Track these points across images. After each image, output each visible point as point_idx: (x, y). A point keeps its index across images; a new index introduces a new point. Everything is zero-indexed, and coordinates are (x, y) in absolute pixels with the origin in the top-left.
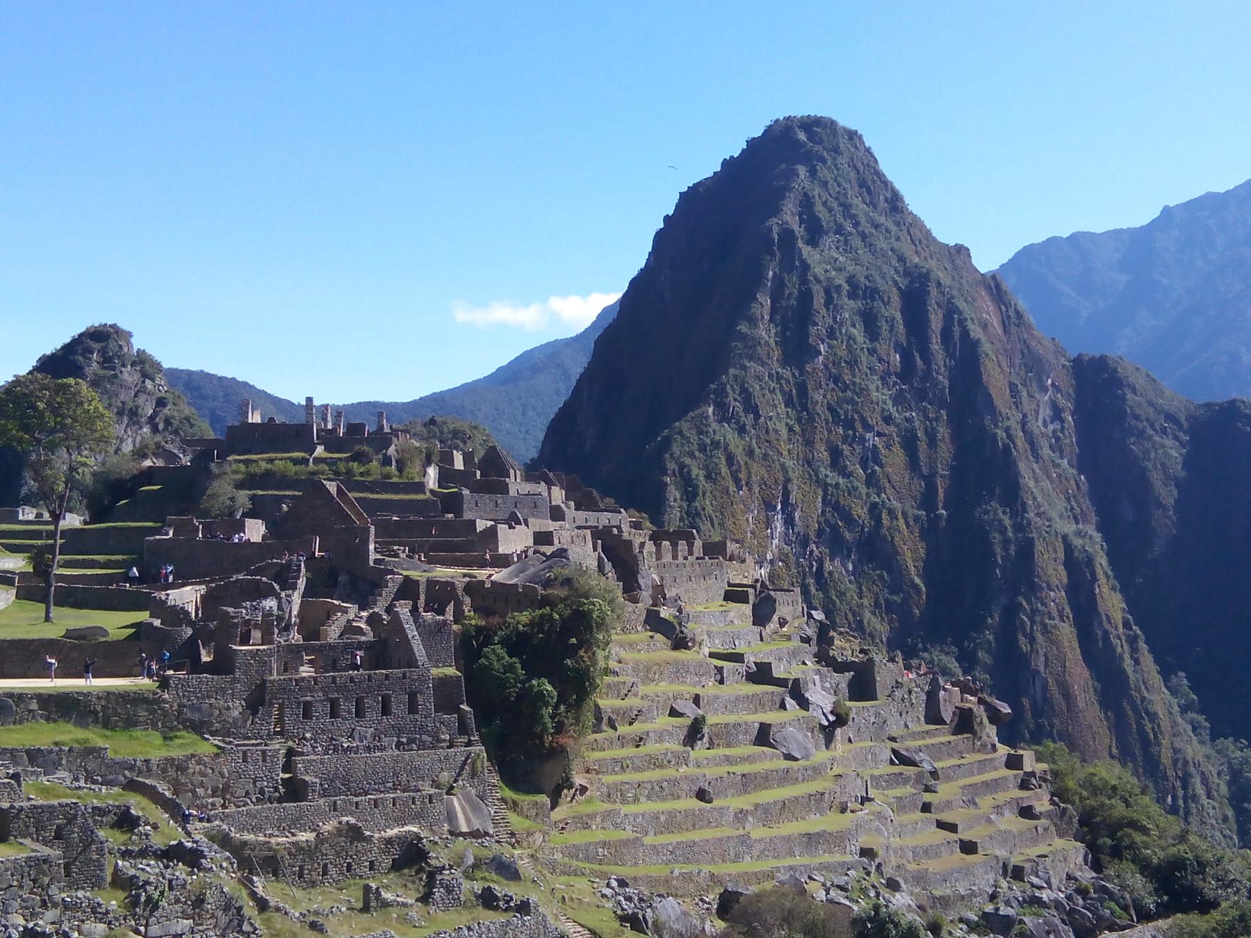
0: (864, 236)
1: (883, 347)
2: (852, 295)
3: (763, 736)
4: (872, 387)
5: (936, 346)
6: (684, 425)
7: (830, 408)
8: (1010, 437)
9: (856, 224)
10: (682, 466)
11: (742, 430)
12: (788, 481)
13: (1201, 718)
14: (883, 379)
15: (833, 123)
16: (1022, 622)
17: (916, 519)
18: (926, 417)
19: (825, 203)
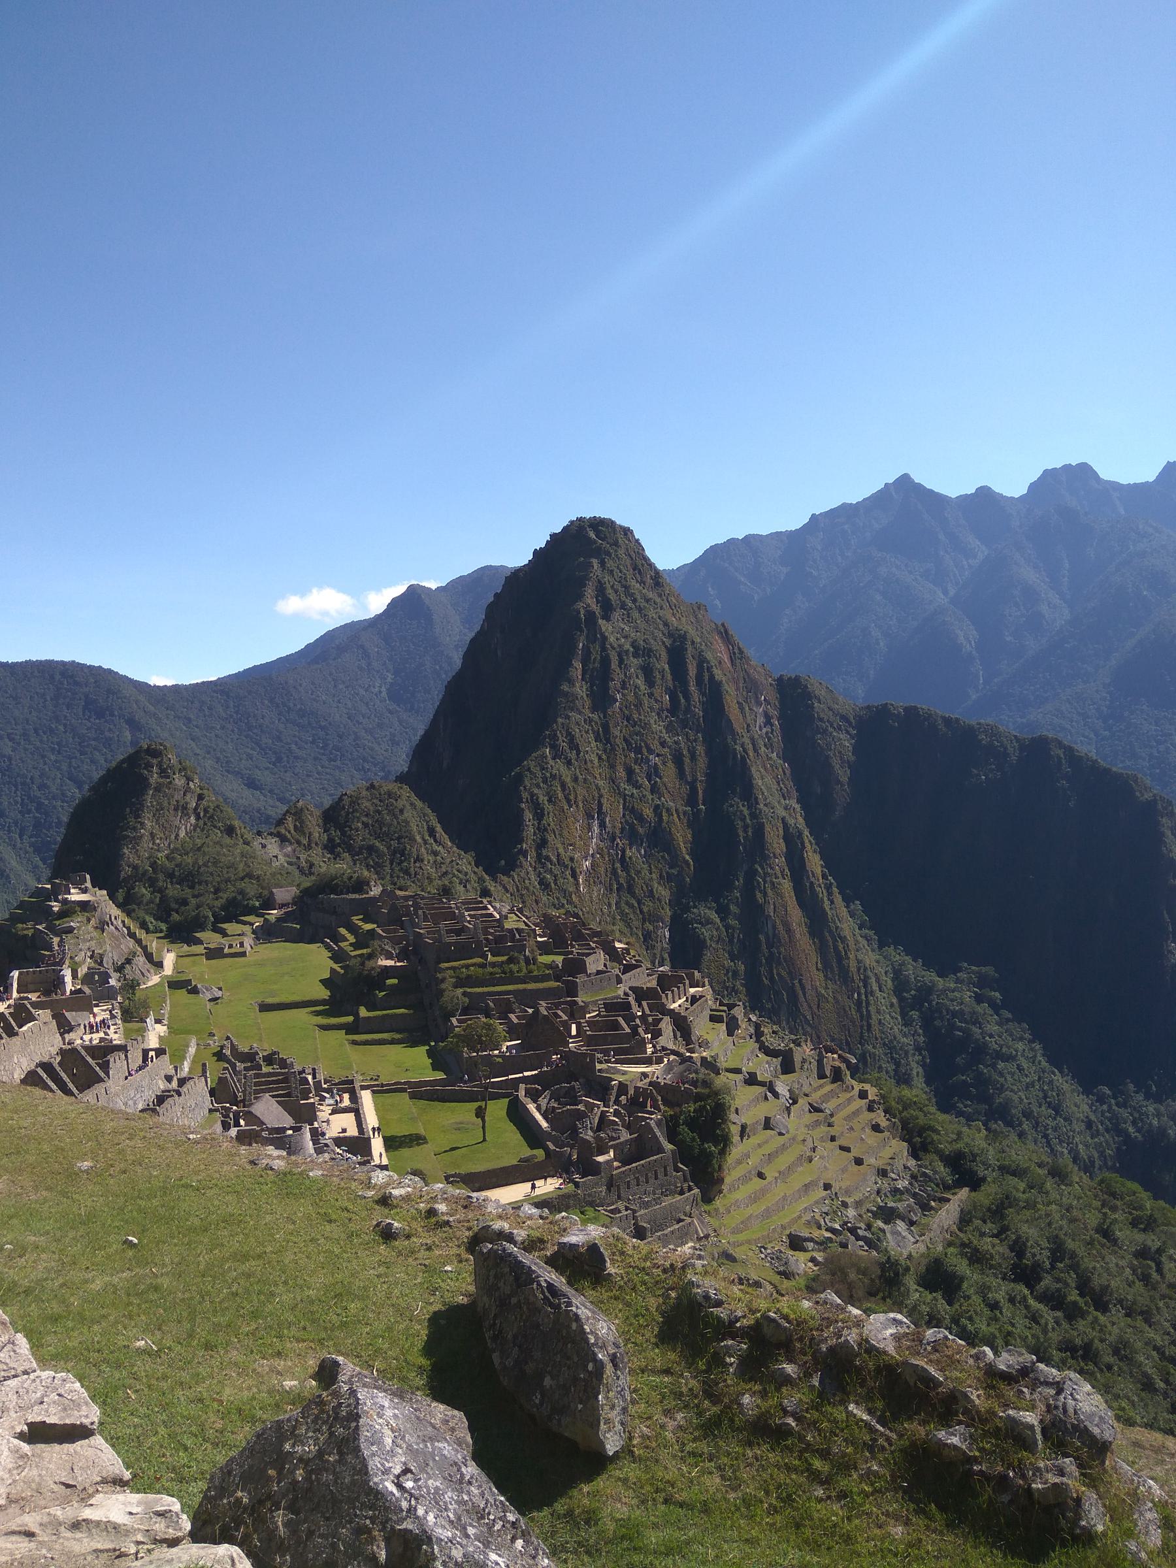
0: (640, 610)
1: (657, 691)
2: (636, 655)
3: (768, 1124)
4: (652, 721)
5: (693, 688)
6: (530, 763)
7: (625, 740)
8: (745, 750)
9: (634, 601)
10: (532, 795)
11: (569, 763)
12: (601, 796)
13: (872, 933)
14: (658, 714)
15: (613, 522)
16: (759, 883)
17: (685, 813)
18: (688, 740)
19: (612, 587)
